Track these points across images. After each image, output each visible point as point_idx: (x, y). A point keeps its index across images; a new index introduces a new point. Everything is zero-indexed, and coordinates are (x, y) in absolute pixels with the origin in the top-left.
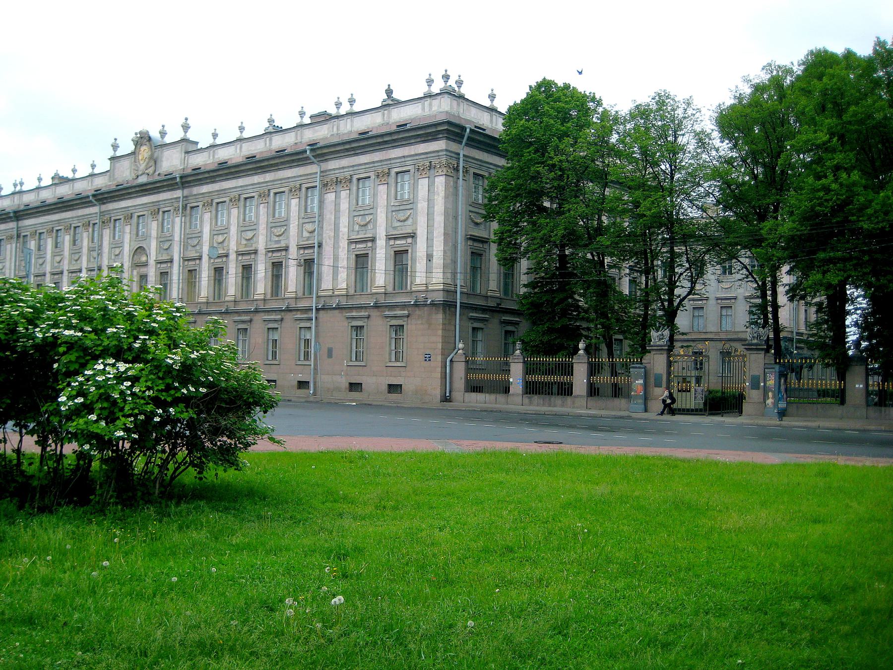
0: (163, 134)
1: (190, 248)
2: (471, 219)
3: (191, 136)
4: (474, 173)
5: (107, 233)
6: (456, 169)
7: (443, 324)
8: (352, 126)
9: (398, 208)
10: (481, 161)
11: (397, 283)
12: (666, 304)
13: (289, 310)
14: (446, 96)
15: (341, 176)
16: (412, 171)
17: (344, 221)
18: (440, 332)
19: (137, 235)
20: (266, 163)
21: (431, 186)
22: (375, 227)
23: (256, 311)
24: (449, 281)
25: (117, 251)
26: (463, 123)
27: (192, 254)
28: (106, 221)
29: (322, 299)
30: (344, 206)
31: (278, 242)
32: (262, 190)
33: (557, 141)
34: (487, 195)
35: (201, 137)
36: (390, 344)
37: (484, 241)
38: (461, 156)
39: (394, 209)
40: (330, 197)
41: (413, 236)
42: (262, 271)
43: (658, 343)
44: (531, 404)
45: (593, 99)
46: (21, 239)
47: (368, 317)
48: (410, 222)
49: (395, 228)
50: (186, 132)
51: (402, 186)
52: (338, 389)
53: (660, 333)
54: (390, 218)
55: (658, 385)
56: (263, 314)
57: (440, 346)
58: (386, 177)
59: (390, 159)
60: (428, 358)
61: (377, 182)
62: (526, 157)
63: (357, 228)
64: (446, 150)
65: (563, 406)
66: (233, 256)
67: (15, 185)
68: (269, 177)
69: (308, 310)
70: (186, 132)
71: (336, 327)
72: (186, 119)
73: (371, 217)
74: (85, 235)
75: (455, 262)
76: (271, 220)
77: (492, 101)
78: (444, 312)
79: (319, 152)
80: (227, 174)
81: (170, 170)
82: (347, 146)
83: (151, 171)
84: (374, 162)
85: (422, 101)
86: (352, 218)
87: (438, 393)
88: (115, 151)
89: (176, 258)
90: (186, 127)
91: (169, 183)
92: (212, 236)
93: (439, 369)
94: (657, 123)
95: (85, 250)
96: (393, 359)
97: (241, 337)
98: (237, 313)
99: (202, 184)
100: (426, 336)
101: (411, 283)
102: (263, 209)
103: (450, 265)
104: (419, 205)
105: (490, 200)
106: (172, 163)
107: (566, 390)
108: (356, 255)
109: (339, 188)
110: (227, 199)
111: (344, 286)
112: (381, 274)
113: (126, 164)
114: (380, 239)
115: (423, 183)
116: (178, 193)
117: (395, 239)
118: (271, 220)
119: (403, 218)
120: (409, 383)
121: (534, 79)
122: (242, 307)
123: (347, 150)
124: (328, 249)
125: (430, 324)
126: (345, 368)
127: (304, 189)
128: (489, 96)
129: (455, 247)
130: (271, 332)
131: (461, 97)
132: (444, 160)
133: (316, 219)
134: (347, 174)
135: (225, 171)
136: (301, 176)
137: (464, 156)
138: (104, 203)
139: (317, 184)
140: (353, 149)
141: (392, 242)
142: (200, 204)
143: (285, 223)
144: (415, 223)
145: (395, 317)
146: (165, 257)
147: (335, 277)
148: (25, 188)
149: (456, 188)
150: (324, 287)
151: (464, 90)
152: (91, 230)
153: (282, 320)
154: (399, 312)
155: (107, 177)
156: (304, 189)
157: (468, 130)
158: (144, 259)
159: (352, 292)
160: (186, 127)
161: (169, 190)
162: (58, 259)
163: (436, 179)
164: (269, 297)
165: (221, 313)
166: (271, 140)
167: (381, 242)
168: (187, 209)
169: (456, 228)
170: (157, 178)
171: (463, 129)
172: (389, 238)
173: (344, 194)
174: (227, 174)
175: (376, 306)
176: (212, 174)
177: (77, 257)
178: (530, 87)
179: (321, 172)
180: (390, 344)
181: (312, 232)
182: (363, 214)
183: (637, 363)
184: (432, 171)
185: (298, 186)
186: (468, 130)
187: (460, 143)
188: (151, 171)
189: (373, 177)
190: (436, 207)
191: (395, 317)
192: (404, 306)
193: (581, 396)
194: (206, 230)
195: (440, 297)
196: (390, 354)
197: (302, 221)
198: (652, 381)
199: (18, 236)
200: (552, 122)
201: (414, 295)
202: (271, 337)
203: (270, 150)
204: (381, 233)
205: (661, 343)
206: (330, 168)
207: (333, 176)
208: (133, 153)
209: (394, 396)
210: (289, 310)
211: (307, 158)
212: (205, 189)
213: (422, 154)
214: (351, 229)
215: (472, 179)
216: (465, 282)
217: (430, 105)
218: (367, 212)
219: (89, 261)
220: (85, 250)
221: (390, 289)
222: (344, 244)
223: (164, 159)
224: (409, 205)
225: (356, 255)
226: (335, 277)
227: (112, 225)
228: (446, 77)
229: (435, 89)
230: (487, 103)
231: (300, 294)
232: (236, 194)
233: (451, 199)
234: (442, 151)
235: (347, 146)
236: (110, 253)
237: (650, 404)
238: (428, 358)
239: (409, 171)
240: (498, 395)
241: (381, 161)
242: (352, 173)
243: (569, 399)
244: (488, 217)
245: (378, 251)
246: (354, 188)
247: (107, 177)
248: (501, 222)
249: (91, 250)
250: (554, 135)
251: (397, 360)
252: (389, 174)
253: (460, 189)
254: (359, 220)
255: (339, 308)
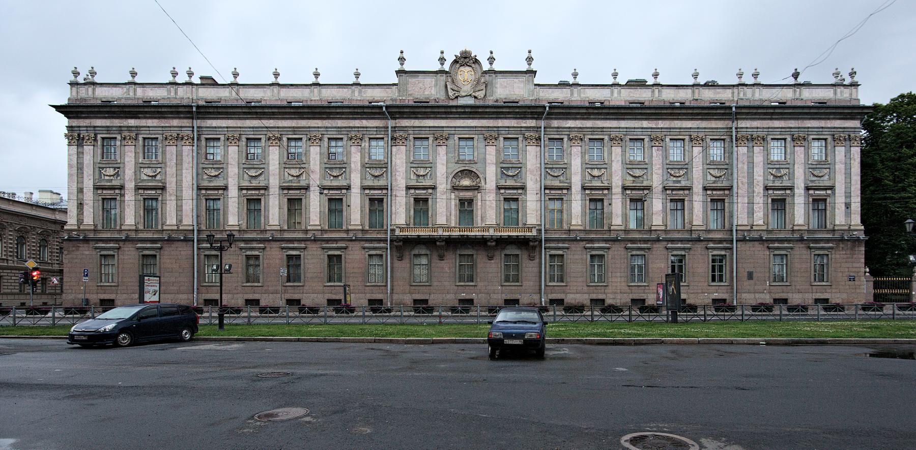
21: (848, 153)
30: (759, 158)
31: (679, 182)
48: (826, 177)
49: (812, 181)
81: (513, 98)
83: (480, 94)
106: (505, 91)
111: (761, 222)
114: (798, 188)
115: (840, 151)
116: (532, 123)
160: (530, 60)
165: (606, 241)
172: (808, 189)
197: (706, 167)
212: (570, 123)
222: (759, 189)
223: (498, 86)
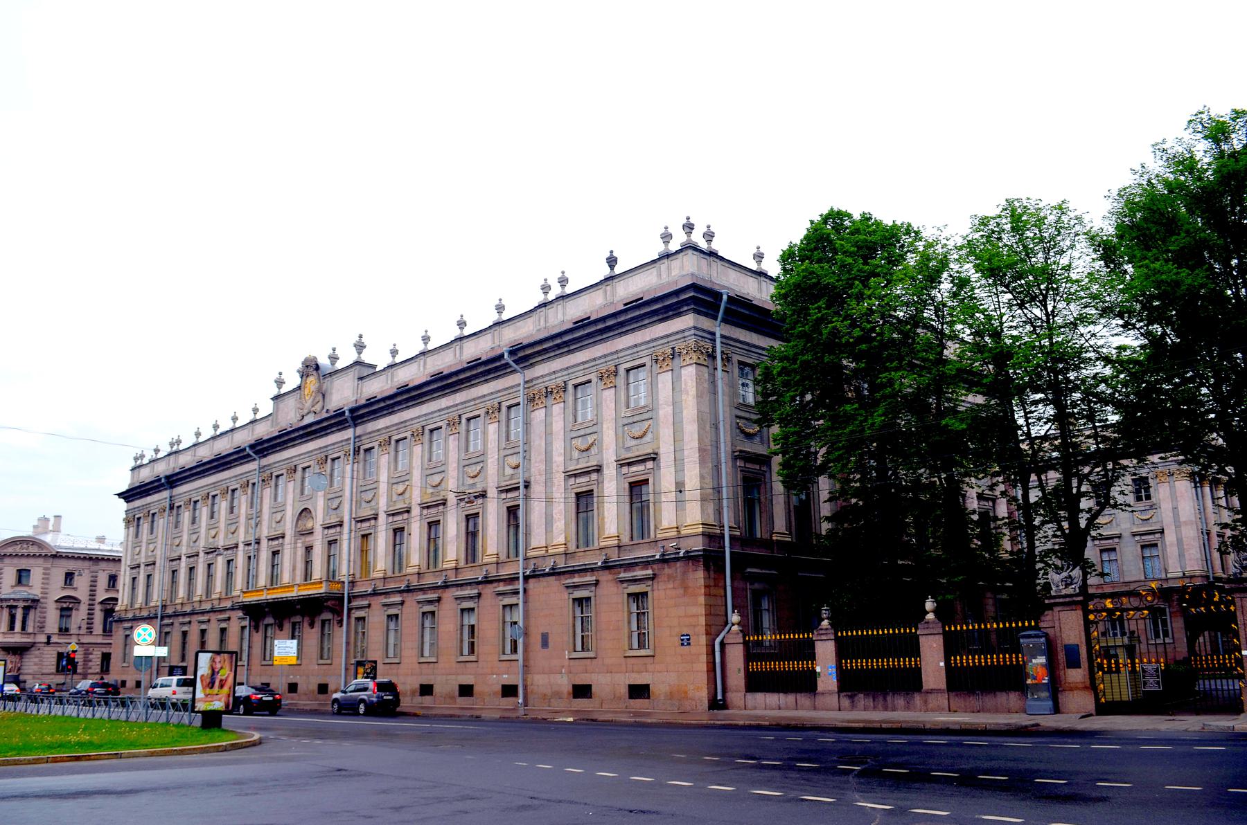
0: (334, 359)
1: (364, 505)
2: (739, 428)
3: (367, 357)
4: (740, 362)
5: (268, 492)
6: (712, 356)
7: (706, 587)
8: (564, 314)
9: (631, 420)
10: (748, 344)
11: (635, 526)
12: (1065, 525)
13: (487, 581)
14: (690, 252)
15: (551, 385)
16: (648, 364)
17: (558, 446)
18: (702, 599)
19: (302, 493)
20: (454, 379)
22: (600, 451)
23: (446, 586)
24: (711, 520)
25: (278, 516)
26: (717, 288)
27: (366, 512)
28: (270, 478)
29: (532, 562)
30: (558, 425)
32: (450, 416)
33: (861, 286)
34: (759, 389)
35: (377, 357)
36: (629, 622)
37: (765, 460)
38: (718, 335)
39: (626, 421)
40: (539, 415)
41: (654, 457)
42: (453, 527)
43: (1064, 592)
44: (853, 706)
45: (908, 231)
46: (175, 511)
47: (597, 583)
49: (628, 449)
50: (360, 353)
51: (637, 388)
52: (557, 695)
53: (1065, 574)
54: (620, 434)
55: (1073, 662)
56: (454, 589)
57: (702, 620)
58: (612, 377)
59: (617, 352)
60: (686, 641)
61: (601, 384)
62: (814, 314)
63: (576, 454)
64: (695, 328)
65: (907, 708)
66: (416, 511)
67: (172, 445)
68: (459, 397)
69: (513, 579)
70: (360, 353)
71: (552, 600)
72: (361, 336)
73: (595, 436)
74: (243, 498)
75: (718, 490)
76: (463, 456)
77: (759, 262)
78: (707, 569)
79: (521, 354)
80: (407, 400)
82: (558, 341)
83: (318, 408)
84: (595, 359)
85: (657, 265)
86: (569, 440)
87: (703, 695)
88: (279, 388)
89: (346, 519)
90: (360, 347)
91: (338, 421)
92: (391, 485)
93: (704, 658)
94: (1015, 252)
95: (243, 519)
96: (635, 645)
97: (427, 624)
98: (423, 590)
99: (377, 418)
100: (681, 606)
101: (656, 527)
102: (452, 443)
103: (712, 495)
104: (661, 412)
105: (765, 395)
106: (344, 395)
107: (910, 682)
108: (577, 494)
109: (550, 401)
110: (408, 434)
111: (561, 540)
112: (612, 518)
113: (291, 402)
115: (665, 379)
116: (349, 433)
117: (629, 464)
118: (463, 456)
119: (637, 434)
120: (660, 680)
121: (816, 213)
122: (428, 580)
123: (558, 346)
124: (537, 489)
125: (686, 588)
126: (566, 663)
127: (504, 409)
128: (755, 256)
129: (717, 468)
130: (466, 615)
131: (713, 254)
132: (691, 341)
133: (521, 449)
134: (560, 381)
135: (409, 396)
136: (499, 391)
137: (722, 336)
138: (265, 456)
139: (520, 400)
140: (566, 344)
141: (625, 470)
142: (376, 444)
143: (481, 459)
144: (656, 438)
145: (635, 581)
146: (334, 520)
147: (550, 527)
148: (182, 447)
149: (713, 383)
150: (534, 544)
151: (716, 246)
152: (249, 492)
153: (479, 595)
154: (639, 573)
155: (269, 423)
156: (504, 409)
157: (725, 297)
158: (309, 525)
159: (572, 548)
160: (360, 347)
161: (339, 430)
162: (213, 532)
163: (684, 371)
164: (462, 564)
165: (401, 592)
166: (461, 348)
167: (610, 471)
168: (360, 451)
169: (717, 442)
170: (325, 415)
171: (718, 296)
172: (622, 464)
173: (557, 409)
174: (407, 400)
175: (607, 566)
176: (388, 402)
177: (233, 528)
178: (812, 222)
179: (526, 382)
180: (629, 622)
181: (517, 467)
182: (584, 435)
183: (1030, 628)
184: (676, 361)
185: (496, 405)
186: (725, 297)
187: (715, 318)
188: (318, 408)
189: (595, 380)
190: (685, 412)
191: (635, 581)
192: (646, 563)
193: (939, 691)
194: (383, 477)
195: (698, 545)
196: (630, 637)
198: (1061, 656)
199: (171, 508)
200: (850, 260)
201: (660, 544)
202: (466, 622)
203: (461, 362)
204: (609, 460)
205: (1070, 591)
206: (537, 375)
207: (541, 386)
208: (299, 388)
209: (639, 704)
210: (487, 581)
211: (507, 365)
213: (662, 338)
214: (568, 458)
215: (736, 370)
216: (737, 522)
217: (669, 268)
218: (588, 431)
219: (247, 532)
220: (243, 519)
221: (626, 539)
222: (559, 478)
224: (648, 413)
225: (577, 494)
226: (550, 527)
227: (273, 483)
228: (689, 227)
229: (674, 246)
230: (753, 266)
231: (503, 557)
232: (419, 426)
233: (706, 398)
234: (689, 329)
235: (558, 341)
236: (270, 519)
237: (1062, 698)
238: (686, 641)
239: (644, 365)
240: (799, 695)
241: (605, 356)
242: (565, 378)
243: (918, 699)
244: (765, 421)
245: (606, 484)
246: (570, 399)
247: (269, 423)
248: (783, 422)
249: (249, 518)
250: (855, 279)
251: (641, 645)
252: (616, 373)
253: (720, 383)
254: (579, 443)
255: (555, 573)
